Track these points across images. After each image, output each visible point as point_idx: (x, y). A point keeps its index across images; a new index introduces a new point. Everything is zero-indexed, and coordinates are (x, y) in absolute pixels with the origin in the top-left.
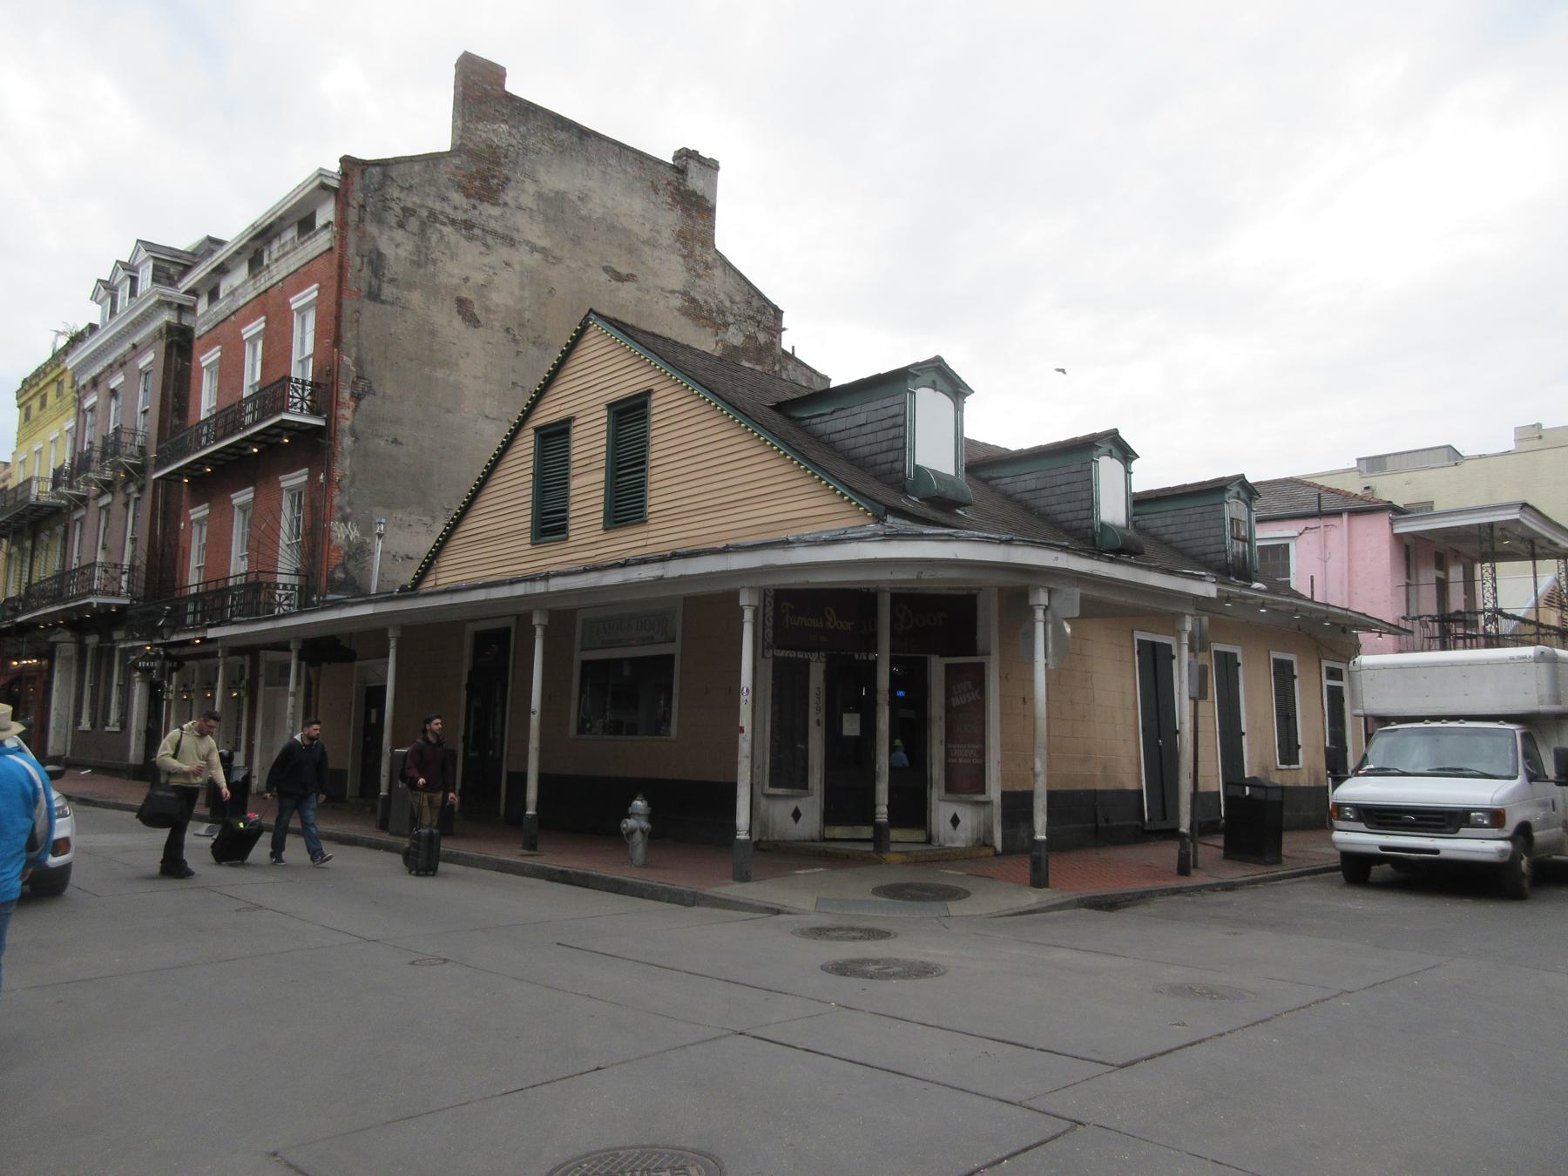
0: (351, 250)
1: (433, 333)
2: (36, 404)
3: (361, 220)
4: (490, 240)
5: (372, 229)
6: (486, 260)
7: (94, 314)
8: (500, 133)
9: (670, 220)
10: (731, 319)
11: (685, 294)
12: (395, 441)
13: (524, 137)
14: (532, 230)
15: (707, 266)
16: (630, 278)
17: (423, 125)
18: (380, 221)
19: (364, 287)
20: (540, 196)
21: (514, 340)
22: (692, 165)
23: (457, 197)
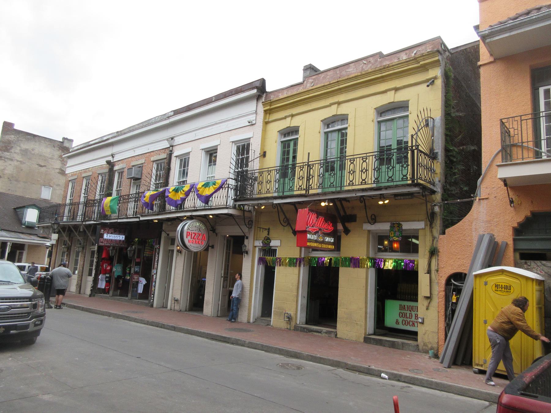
4: (6, 160)
8: (12, 137)
11: (60, 169)
14: (18, 157)
16: (44, 166)
20: (21, 150)
21: (10, 180)
22: (66, 141)
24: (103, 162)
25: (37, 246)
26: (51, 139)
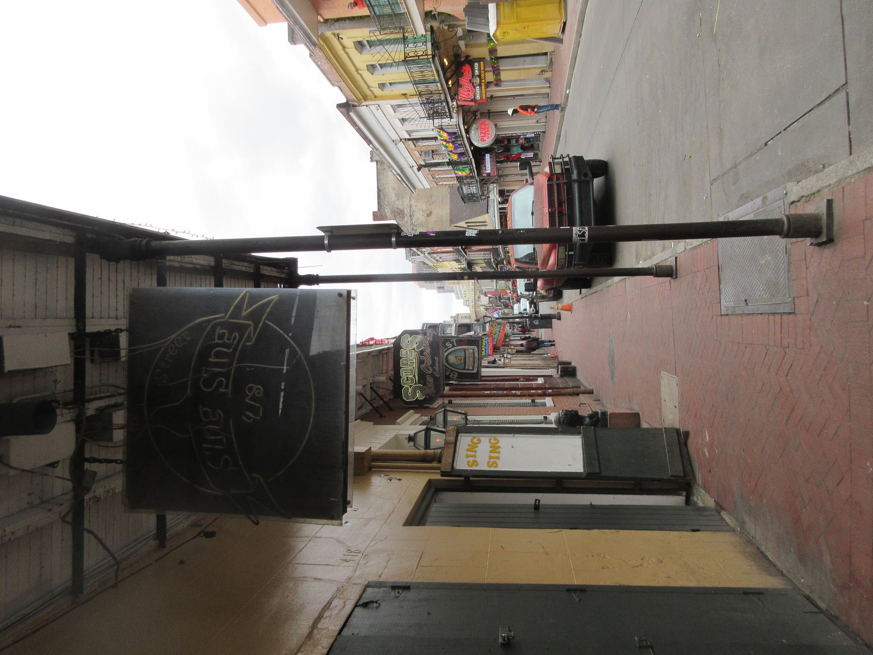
14: (406, 201)
23: (406, 219)
24: (420, 174)
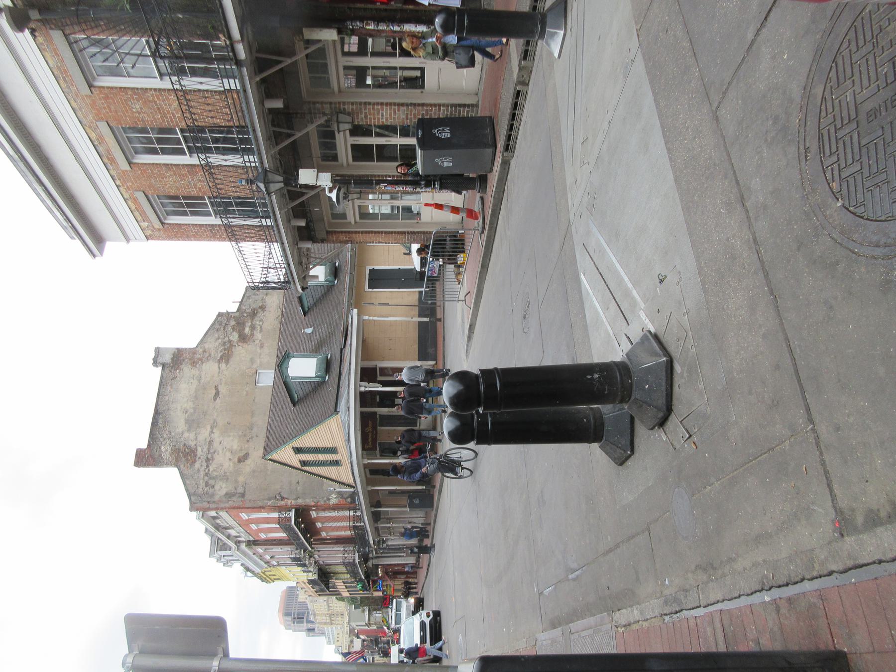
0: (227, 505)
1: (254, 471)
2: (272, 577)
3: (214, 502)
4: (212, 451)
5: (217, 498)
6: (221, 452)
7: (237, 566)
8: (166, 450)
9: (187, 370)
10: (227, 339)
11: (219, 362)
12: (298, 483)
13: (165, 439)
14: (204, 433)
15: (204, 351)
16: (216, 388)
17: (168, 479)
18: (213, 495)
19: (240, 499)
20: (189, 430)
21: (252, 438)
22: (159, 360)
23: (197, 465)
25: (364, 341)
26: (160, 385)
